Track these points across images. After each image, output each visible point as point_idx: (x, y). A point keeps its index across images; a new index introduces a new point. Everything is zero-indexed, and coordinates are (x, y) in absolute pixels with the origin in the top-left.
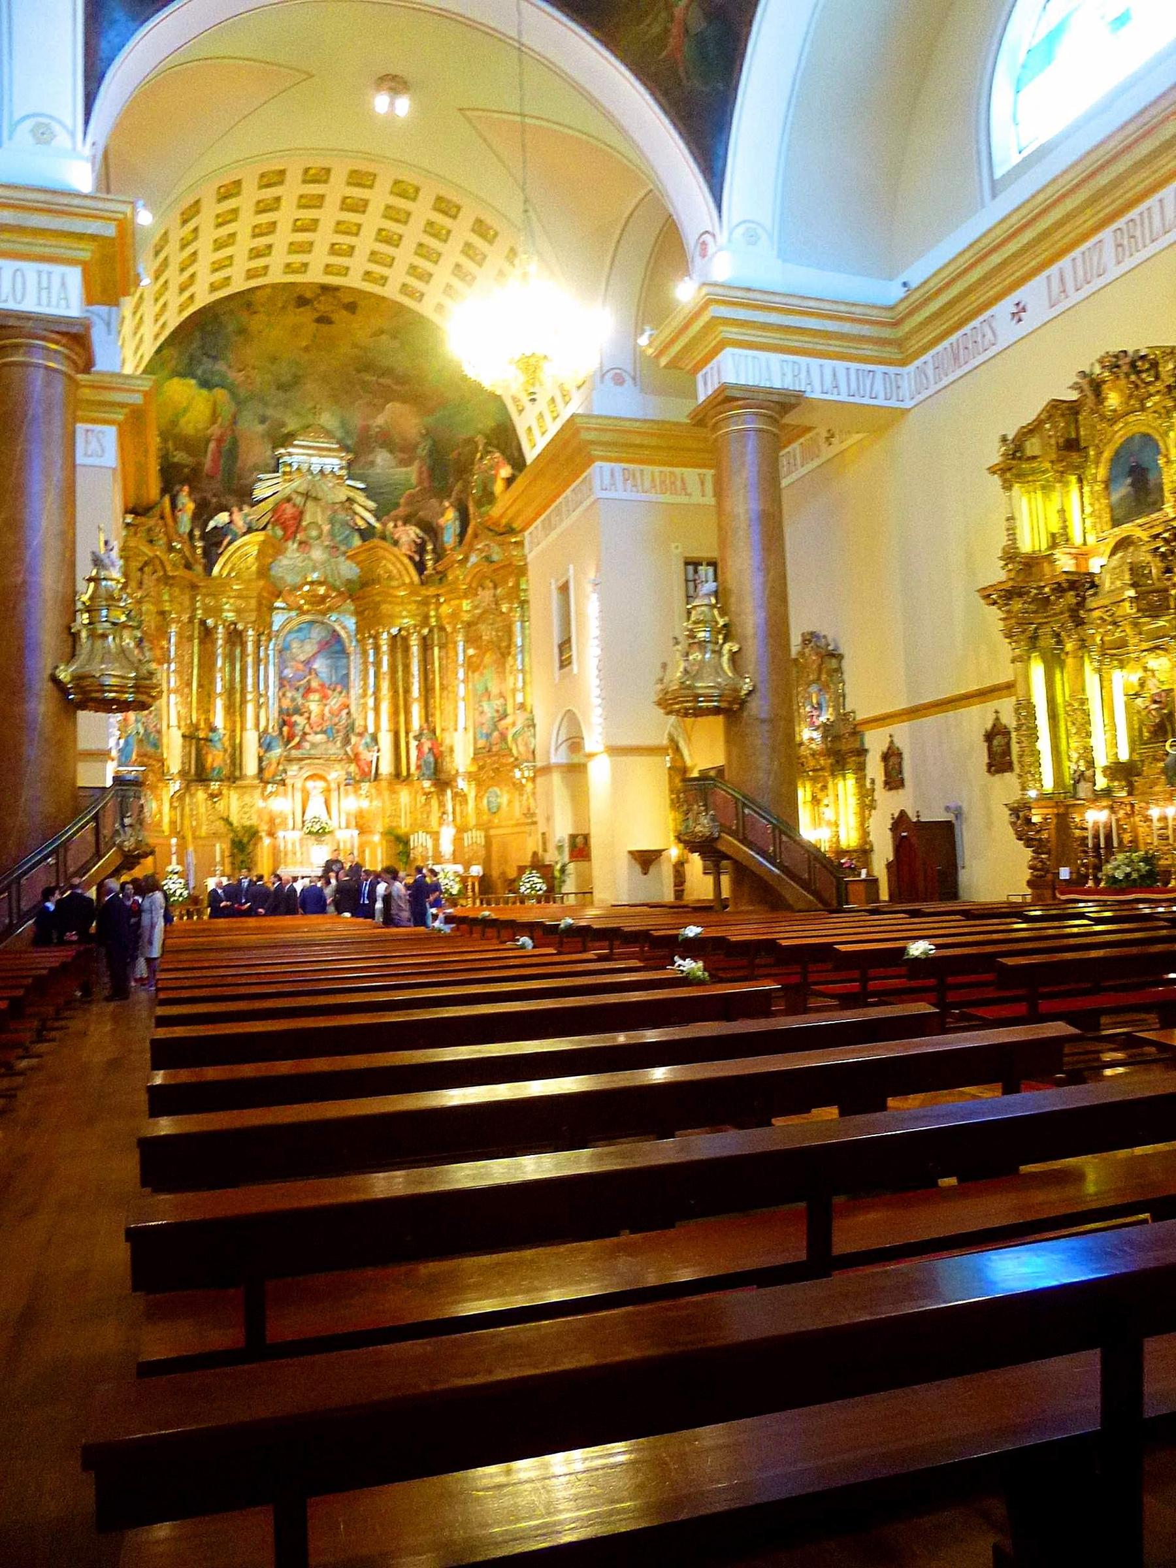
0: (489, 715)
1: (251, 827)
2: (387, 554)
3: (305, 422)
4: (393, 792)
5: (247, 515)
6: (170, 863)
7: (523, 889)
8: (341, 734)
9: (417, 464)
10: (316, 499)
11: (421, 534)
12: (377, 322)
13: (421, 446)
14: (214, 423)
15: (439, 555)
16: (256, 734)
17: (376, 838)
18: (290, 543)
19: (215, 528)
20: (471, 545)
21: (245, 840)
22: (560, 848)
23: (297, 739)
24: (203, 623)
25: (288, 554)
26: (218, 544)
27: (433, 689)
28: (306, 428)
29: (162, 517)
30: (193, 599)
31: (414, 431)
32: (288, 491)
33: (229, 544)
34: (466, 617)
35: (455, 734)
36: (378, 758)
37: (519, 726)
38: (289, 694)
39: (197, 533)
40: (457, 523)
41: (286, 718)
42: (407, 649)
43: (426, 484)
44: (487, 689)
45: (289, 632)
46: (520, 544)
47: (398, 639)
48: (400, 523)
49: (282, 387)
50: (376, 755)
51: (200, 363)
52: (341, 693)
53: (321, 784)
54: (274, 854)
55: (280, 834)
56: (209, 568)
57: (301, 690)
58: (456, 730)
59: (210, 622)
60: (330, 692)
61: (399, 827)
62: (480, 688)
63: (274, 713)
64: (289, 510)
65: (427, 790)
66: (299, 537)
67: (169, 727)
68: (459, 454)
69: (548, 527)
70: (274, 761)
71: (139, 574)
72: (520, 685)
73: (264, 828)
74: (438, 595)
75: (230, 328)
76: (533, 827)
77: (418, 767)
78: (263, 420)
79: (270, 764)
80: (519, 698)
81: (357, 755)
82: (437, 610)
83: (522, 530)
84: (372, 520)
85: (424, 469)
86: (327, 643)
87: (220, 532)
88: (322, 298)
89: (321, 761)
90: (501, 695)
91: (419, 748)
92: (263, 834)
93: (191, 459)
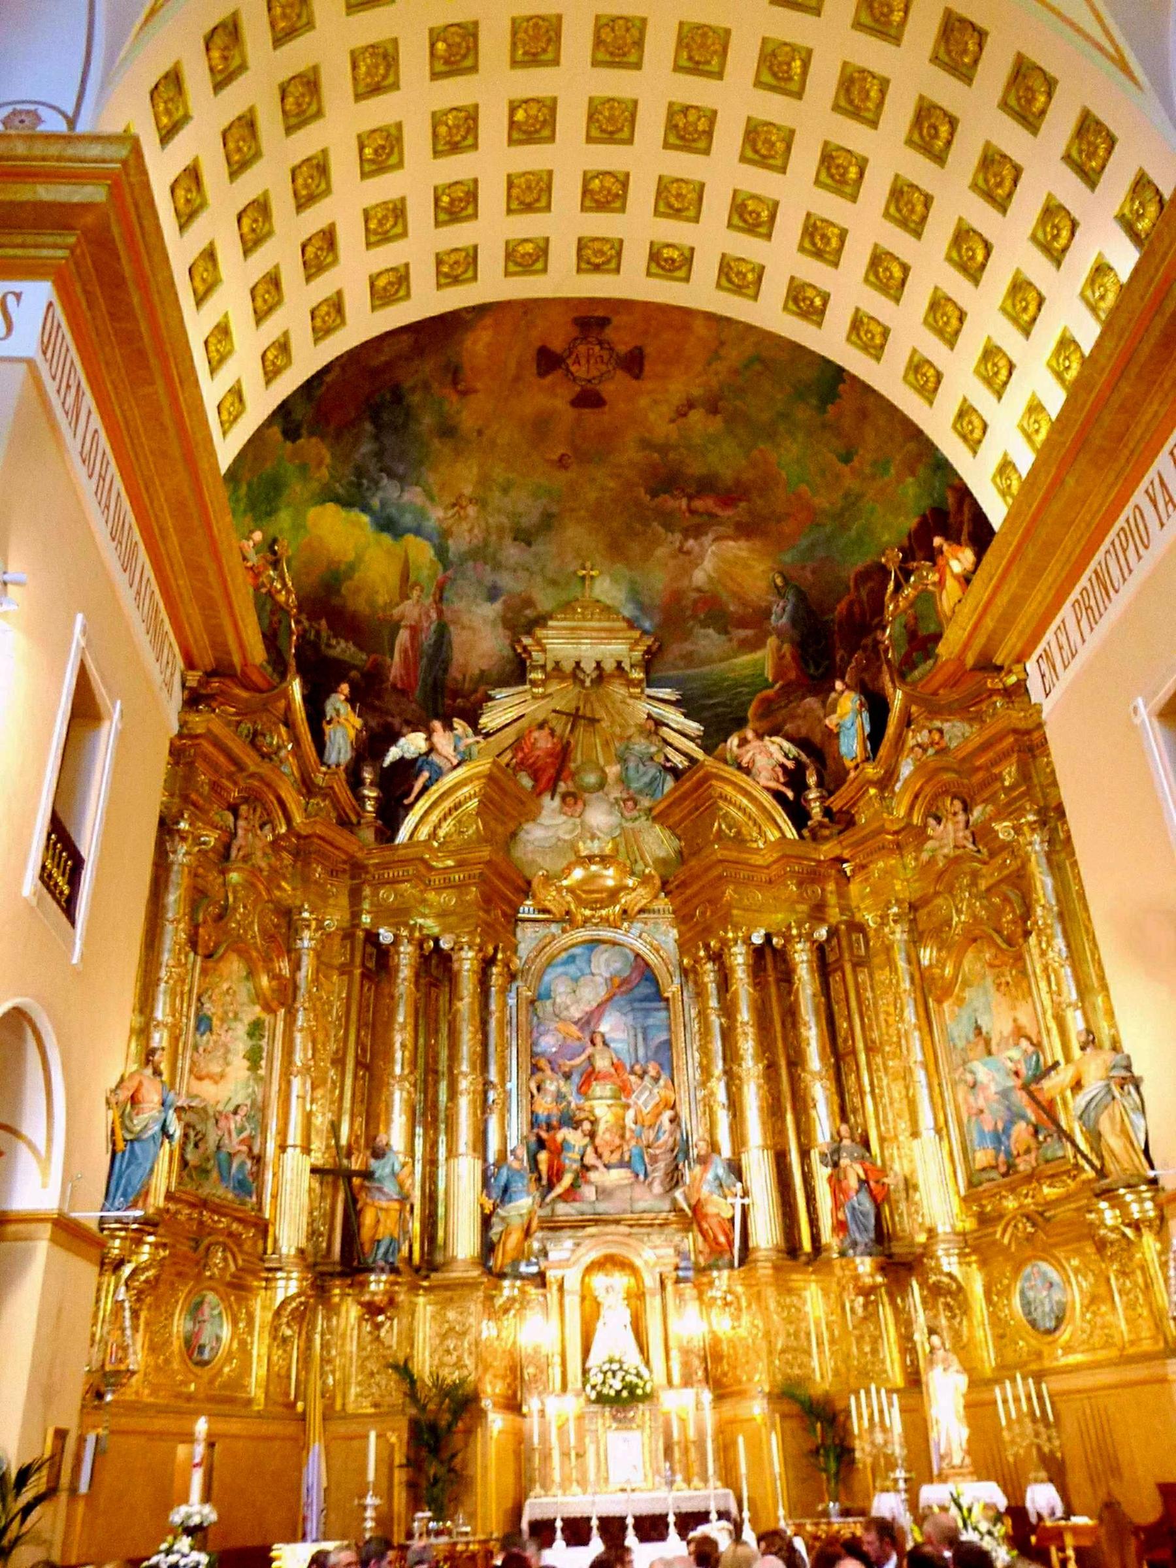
0: (993, 1088)
1: (455, 1386)
2: (729, 790)
3: (564, 596)
4: (786, 1289)
6: (185, 1499)
8: (661, 1165)
11: (794, 751)
12: (678, 388)
14: (405, 596)
15: (834, 777)
16: (479, 1165)
17: (758, 1409)
18: (546, 799)
19: (401, 762)
21: (445, 1419)
23: (567, 1180)
24: (372, 937)
25: (546, 818)
26: (408, 795)
27: (854, 1052)
28: (567, 607)
29: (289, 723)
30: (355, 896)
31: (763, 584)
32: (541, 717)
33: (425, 789)
36: (745, 1211)
37: (1093, 1086)
38: (551, 1087)
39: (368, 776)
40: (865, 715)
41: (544, 1135)
42: (787, 976)
43: (792, 675)
44: (978, 1030)
46: (1019, 690)
47: (768, 951)
48: (750, 735)
49: (525, 537)
50: (738, 1202)
52: (656, 1080)
53: (621, 1281)
54: (518, 1455)
55: (532, 1405)
57: (576, 1078)
58: (915, 1134)
59: (386, 936)
60: (633, 1078)
61: (809, 1378)
62: (960, 1030)
64: (543, 742)
65: (868, 1281)
66: (562, 787)
67: (283, 1148)
68: (851, 604)
69: (1090, 612)
70: (517, 1223)
71: (231, 818)
73: (492, 1390)
74: (841, 860)
75: (428, 420)
77: (840, 1227)
78: (493, 594)
79: (506, 1233)
81: (696, 1208)
82: (842, 894)
83: (1021, 659)
84: (699, 754)
85: (786, 647)
86: (625, 981)
87: (407, 768)
88: (582, 349)
89: (623, 1229)
90: (1019, 1033)
91: (837, 1183)
92: (486, 1403)
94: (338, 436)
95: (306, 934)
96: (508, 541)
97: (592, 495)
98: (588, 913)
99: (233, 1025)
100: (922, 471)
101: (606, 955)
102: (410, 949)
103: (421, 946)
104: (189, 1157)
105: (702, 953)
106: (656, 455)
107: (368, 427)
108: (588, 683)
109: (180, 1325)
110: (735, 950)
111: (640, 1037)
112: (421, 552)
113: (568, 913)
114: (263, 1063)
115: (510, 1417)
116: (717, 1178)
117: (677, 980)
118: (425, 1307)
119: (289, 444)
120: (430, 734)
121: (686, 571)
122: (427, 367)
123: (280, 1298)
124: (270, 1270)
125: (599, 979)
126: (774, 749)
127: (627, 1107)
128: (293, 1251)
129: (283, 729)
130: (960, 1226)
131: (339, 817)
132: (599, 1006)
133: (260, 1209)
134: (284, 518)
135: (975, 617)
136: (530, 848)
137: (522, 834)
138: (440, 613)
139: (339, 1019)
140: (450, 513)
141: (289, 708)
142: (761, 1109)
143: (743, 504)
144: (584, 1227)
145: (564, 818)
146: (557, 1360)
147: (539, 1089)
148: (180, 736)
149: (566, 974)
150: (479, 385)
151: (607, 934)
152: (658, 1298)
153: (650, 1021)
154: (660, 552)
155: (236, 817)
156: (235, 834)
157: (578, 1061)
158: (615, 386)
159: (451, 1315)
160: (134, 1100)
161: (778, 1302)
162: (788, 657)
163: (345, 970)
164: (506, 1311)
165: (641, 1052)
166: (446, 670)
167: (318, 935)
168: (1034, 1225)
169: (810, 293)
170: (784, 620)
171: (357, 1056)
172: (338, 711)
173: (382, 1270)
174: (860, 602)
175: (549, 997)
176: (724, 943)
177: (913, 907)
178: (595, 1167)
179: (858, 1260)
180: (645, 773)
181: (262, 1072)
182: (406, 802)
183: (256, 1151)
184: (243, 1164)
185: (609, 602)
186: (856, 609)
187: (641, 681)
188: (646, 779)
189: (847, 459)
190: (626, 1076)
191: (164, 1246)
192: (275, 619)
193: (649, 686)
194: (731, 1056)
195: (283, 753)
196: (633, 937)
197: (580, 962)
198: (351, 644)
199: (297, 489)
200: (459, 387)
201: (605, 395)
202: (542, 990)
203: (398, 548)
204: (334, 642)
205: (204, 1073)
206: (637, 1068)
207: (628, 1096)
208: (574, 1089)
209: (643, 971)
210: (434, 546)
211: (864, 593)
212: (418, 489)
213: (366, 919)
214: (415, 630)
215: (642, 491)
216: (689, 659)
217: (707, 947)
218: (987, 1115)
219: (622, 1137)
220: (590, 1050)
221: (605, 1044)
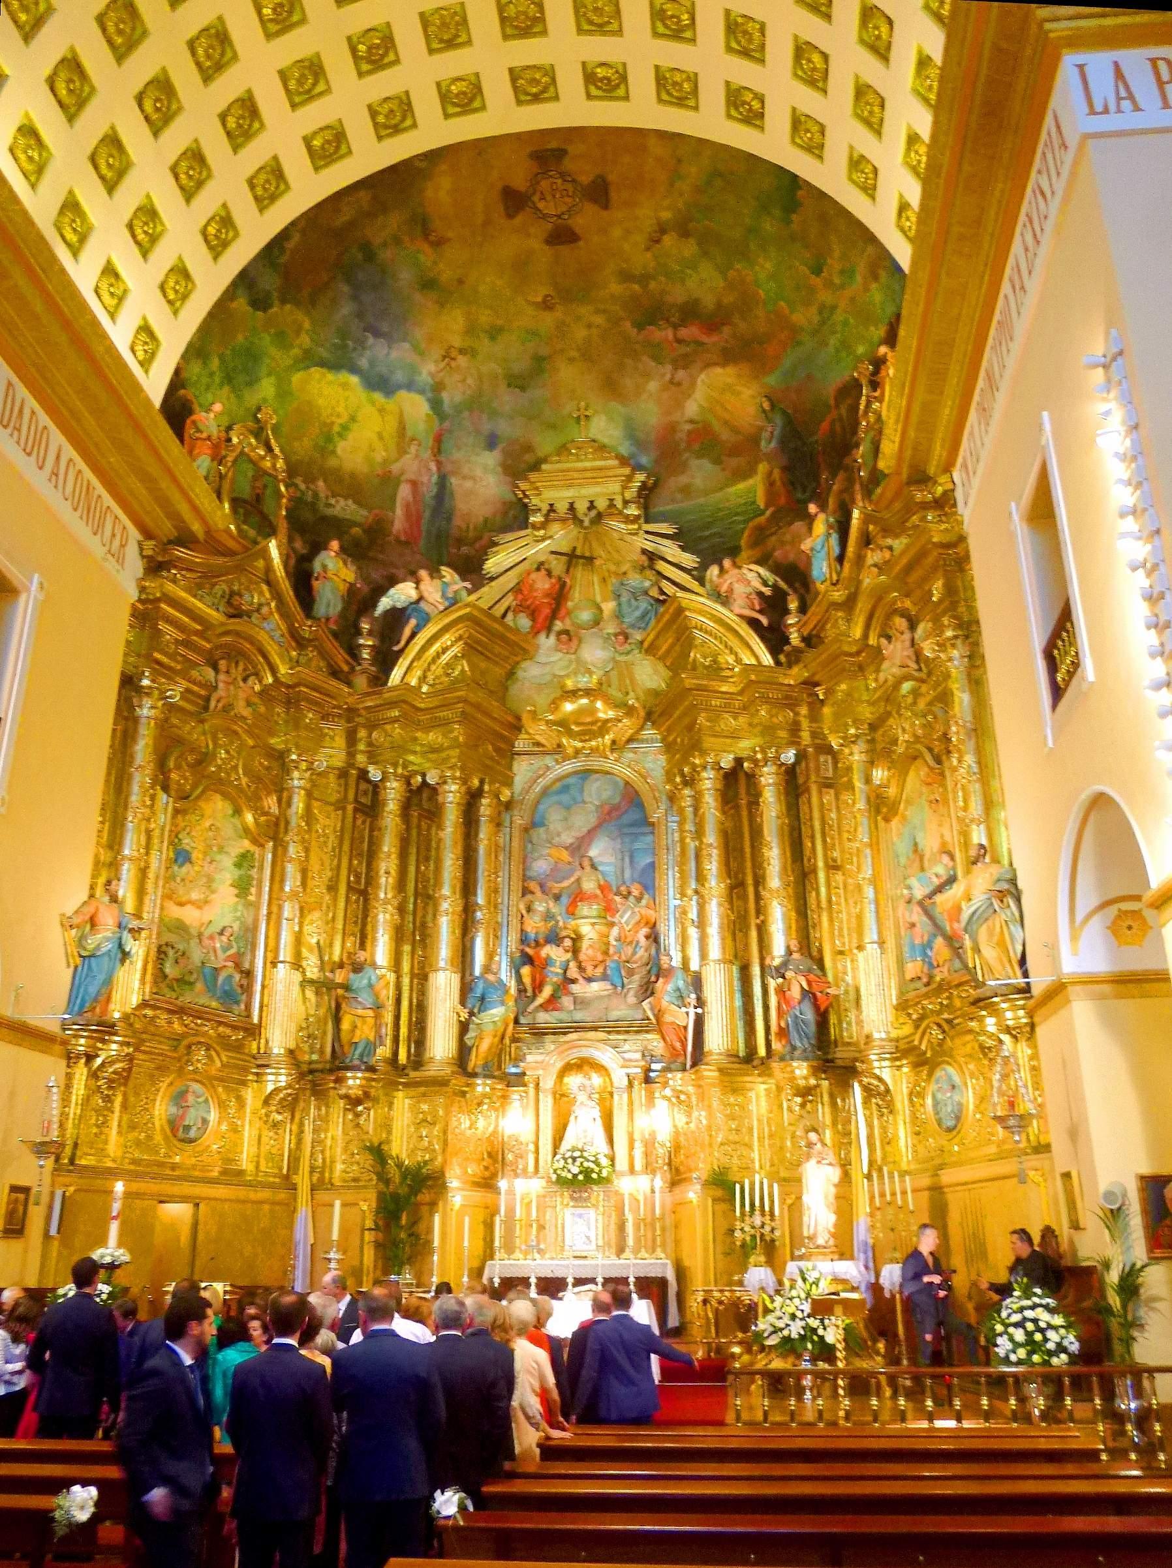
5: (446, 584)
7: (1003, 1346)
8: (636, 977)
9: (762, 468)
10: (590, 560)
13: (765, 435)
14: (402, 451)
17: (693, 1194)
18: (542, 637)
20: (860, 560)
22: (1114, 1216)
23: (547, 991)
24: (363, 775)
25: (541, 658)
27: (814, 871)
31: (752, 410)
33: (413, 635)
34: (867, 713)
35: (861, 956)
36: (699, 1022)
37: (979, 899)
38: (540, 907)
39: (365, 626)
43: (782, 501)
45: (545, 792)
46: (945, 504)
50: (692, 1011)
51: (361, 343)
52: (639, 899)
53: (597, 1080)
55: (503, 1184)
56: (380, 679)
57: (565, 900)
58: (860, 948)
59: (375, 774)
60: (618, 899)
62: (903, 847)
63: (510, 942)
64: (542, 584)
65: (802, 1083)
66: (558, 625)
71: (210, 673)
72: (976, 808)
75: (405, 276)
76: (1034, 1161)
78: (491, 442)
79: (480, 1038)
80: (978, 836)
81: (659, 1015)
82: (814, 717)
83: (948, 468)
85: (777, 474)
87: (397, 616)
88: (545, 184)
91: (781, 991)
92: (454, 1183)
93: (365, 513)
94: (313, 302)
95: (296, 774)
96: (503, 387)
97: (580, 333)
98: (579, 745)
99: (218, 857)
100: (883, 274)
101: (598, 784)
102: (395, 784)
103: (409, 784)
104: (168, 970)
105: (678, 779)
106: (636, 287)
107: (346, 289)
108: (586, 523)
109: (161, 1109)
110: (704, 775)
111: (627, 860)
112: (416, 407)
113: (559, 746)
114: (253, 890)
115: (479, 1195)
116: (679, 989)
117: (663, 807)
118: (402, 1102)
119: (260, 314)
120: (418, 582)
121: (679, 404)
122: (394, 221)
123: (270, 1087)
124: (259, 1066)
125: (591, 807)
126: (751, 576)
127: (612, 924)
128: (282, 1051)
129: (265, 587)
130: (894, 1034)
131: (330, 666)
132: (589, 832)
133: (249, 1016)
134: (267, 388)
135: (900, 427)
136: (527, 684)
137: (520, 674)
138: (439, 464)
139: (333, 850)
140: (442, 365)
141: (269, 569)
142: (721, 927)
143: (726, 330)
144: (565, 1034)
145: (560, 655)
146: (532, 1147)
147: (529, 910)
148: (140, 600)
149: (560, 803)
150: (450, 234)
151: (596, 763)
152: (625, 1096)
153: (637, 845)
154: (653, 386)
155: (216, 668)
156: (216, 687)
157: (566, 884)
158: (585, 218)
159: (425, 1107)
160: (93, 922)
161: (721, 1100)
162: (778, 483)
163: (340, 806)
164: (480, 1104)
165: (627, 874)
166: (449, 519)
167: (307, 775)
168: (944, 1032)
169: (748, 97)
170: (773, 444)
171: (349, 882)
172: (325, 567)
173: (359, 1069)
174: (841, 419)
175: (542, 824)
176: (694, 767)
177: (873, 727)
178: (573, 981)
179: (795, 1064)
180: (637, 608)
181: (252, 898)
182: (396, 648)
183: (247, 966)
184: (230, 977)
185: (606, 441)
186: (838, 427)
187: (637, 517)
188: (638, 613)
189: (817, 270)
190: (611, 896)
191: (128, 1044)
192: (258, 484)
193: (647, 521)
194: (700, 878)
195: (265, 610)
196: (622, 768)
197: (574, 791)
198: (350, 502)
199: (276, 357)
200: (432, 238)
201: (578, 230)
202: (537, 819)
203: (390, 404)
204: (333, 501)
205: (184, 899)
206: (623, 888)
207: (613, 916)
208: (564, 910)
209: (631, 798)
210: (429, 400)
211: (843, 411)
212: (407, 345)
213: (361, 759)
214: (414, 484)
215: (628, 324)
216: (686, 490)
217: (683, 775)
218: (918, 929)
219: (606, 953)
220: (578, 874)
221: (594, 867)
